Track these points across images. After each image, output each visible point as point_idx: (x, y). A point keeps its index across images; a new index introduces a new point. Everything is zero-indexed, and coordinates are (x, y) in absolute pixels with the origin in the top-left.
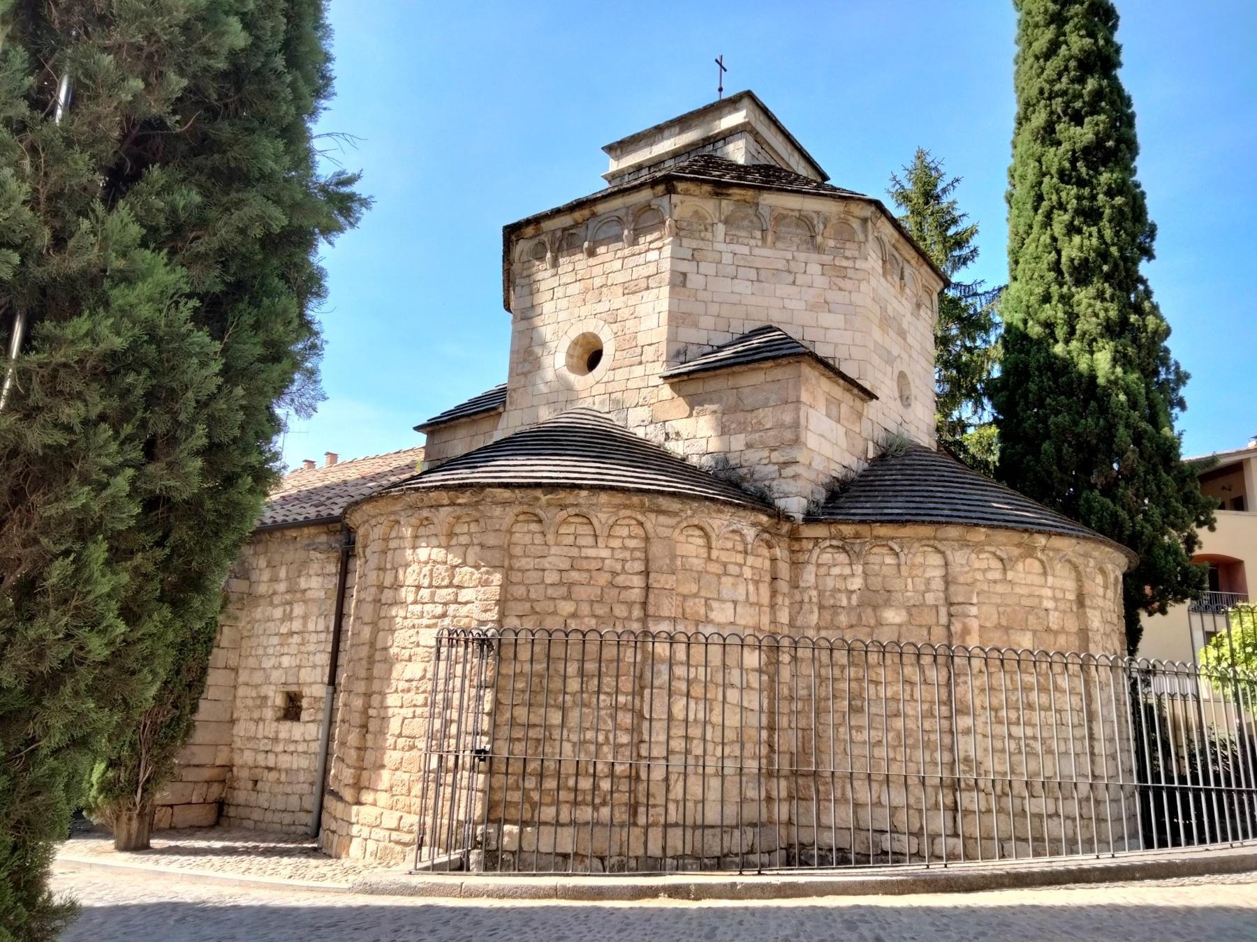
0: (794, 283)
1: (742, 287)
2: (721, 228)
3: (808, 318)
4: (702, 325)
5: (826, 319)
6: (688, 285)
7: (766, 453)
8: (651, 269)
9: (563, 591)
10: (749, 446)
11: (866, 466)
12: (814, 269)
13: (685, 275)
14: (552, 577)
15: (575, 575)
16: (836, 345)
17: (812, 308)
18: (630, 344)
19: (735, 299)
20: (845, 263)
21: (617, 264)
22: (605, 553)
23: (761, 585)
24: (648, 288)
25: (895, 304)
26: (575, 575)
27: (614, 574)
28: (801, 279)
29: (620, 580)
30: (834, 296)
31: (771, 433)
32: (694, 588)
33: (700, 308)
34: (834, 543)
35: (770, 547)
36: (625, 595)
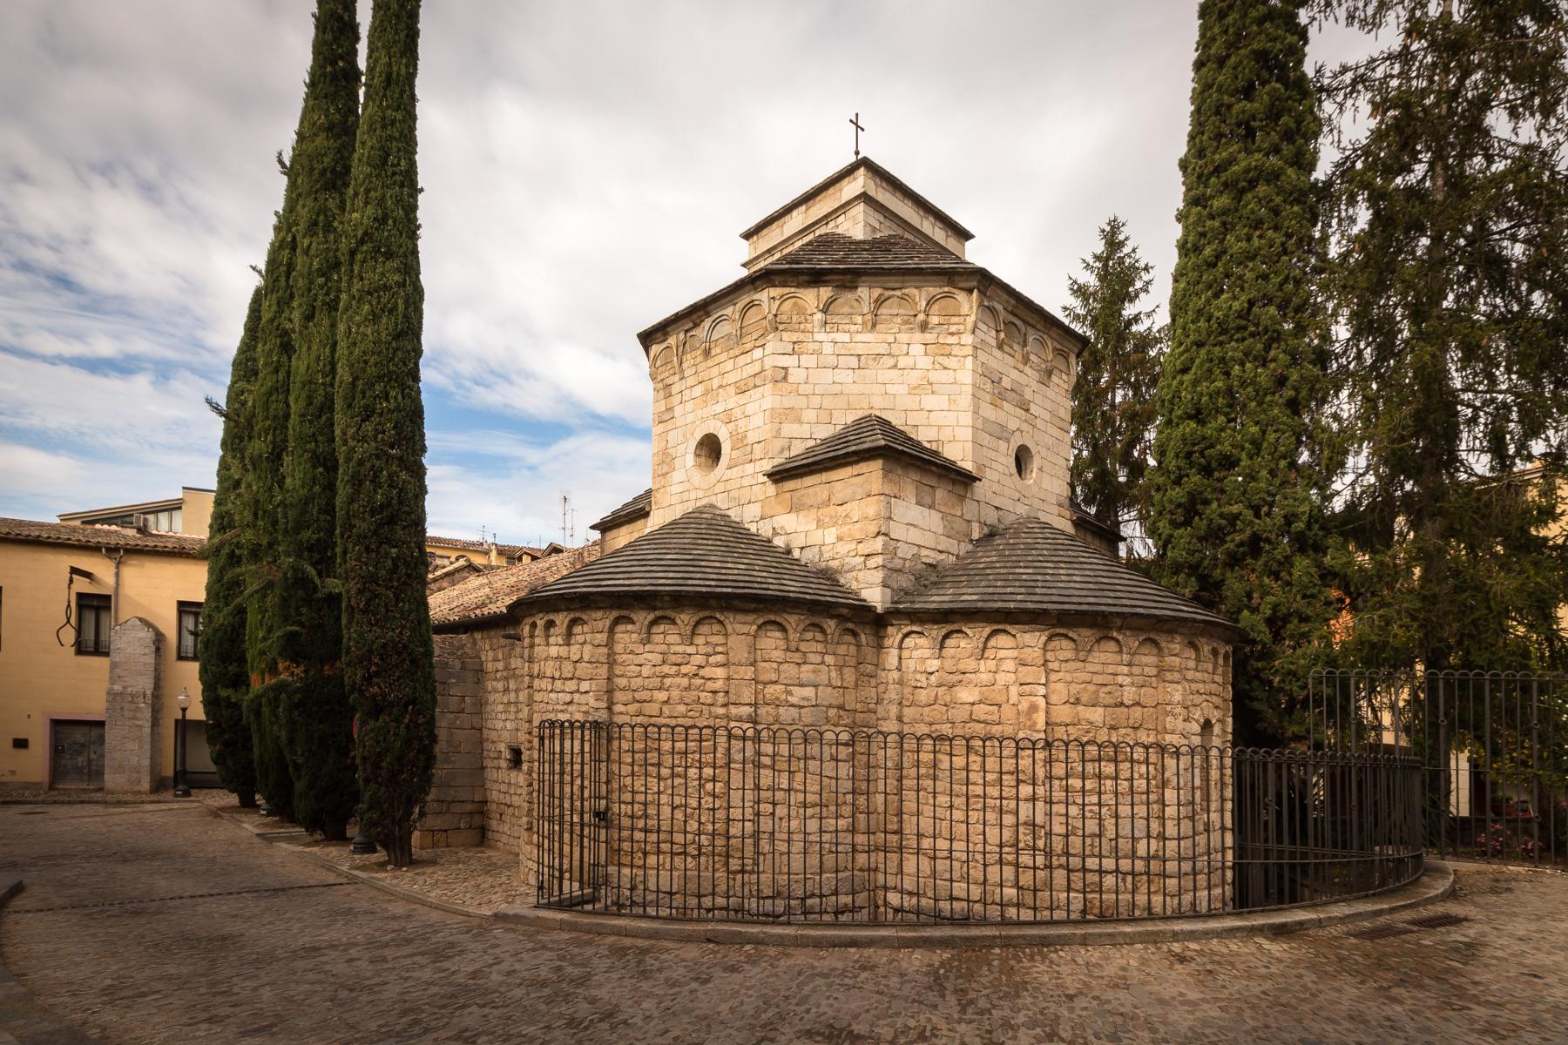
1: (845, 376)
3: (910, 402)
4: (805, 419)
5: (929, 401)
6: (791, 379)
7: (853, 546)
8: (756, 368)
9: (656, 682)
10: (840, 539)
13: (786, 369)
14: (646, 671)
15: (666, 669)
16: (939, 427)
18: (740, 440)
19: (837, 388)
21: (729, 365)
24: (756, 386)
25: (1015, 374)
26: (666, 669)
27: (700, 667)
28: (902, 362)
29: (705, 672)
31: (857, 526)
32: (774, 677)
33: (802, 402)
34: (915, 628)
35: (855, 634)
36: (710, 685)
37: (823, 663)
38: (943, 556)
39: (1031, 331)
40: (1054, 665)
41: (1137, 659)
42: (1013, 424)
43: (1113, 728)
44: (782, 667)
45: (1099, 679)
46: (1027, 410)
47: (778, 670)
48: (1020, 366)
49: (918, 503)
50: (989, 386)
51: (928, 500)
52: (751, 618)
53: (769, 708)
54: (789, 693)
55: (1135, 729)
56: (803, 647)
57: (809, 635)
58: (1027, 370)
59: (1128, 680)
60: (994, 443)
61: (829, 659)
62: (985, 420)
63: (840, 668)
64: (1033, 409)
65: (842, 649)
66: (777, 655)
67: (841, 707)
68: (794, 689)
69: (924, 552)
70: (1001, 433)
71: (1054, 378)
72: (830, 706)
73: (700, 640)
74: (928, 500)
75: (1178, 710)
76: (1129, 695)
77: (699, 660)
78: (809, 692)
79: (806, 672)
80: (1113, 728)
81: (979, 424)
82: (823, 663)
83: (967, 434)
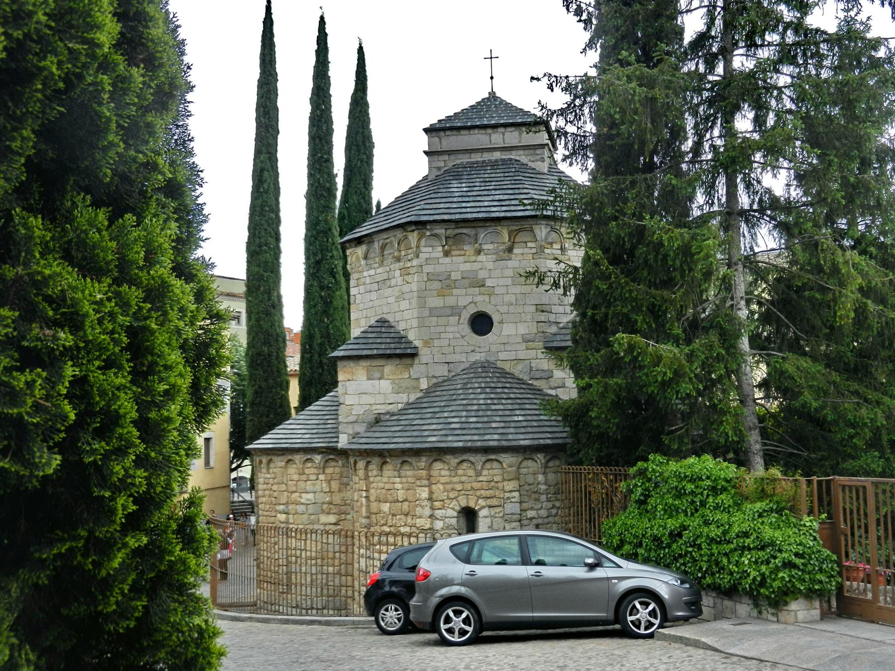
0: (390, 287)
1: (374, 296)
2: (363, 262)
3: (395, 308)
5: (404, 305)
11: (420, 395)
12: (398, 273)
17: (399, 299)
20: (409, 264)
22: (269, 476)
23: (333, 483)
30: (406, 288)
32: (294, 489)
37: (317, 479)
38: (391, 406)
39: (480, 230)
40: (371, 479)
41: (403, 473)
42: (462, 302)
43: (394, 515)
44: (299, 483)
45: (387, 486)
46: (483, 285)
47: (296, 485)
48: (473, 258)
49: (369, 379)
50: (436, 285)
51: (377, 375)
52: (282, 458)
53: (293, 506)
54: (301, 497)
55: (406, 515)
56: (307, 471)
57: (309, 465)
58: (482, 258)
59: (399, 486)
60: (443, 320)
61: (321, 477)
62: (431, 309)
63: (329, 482)
64: (489, 283)
65: (329, 470)
66: (296, 477)
67: (330, 503)
68: (303, 495)
69: (374, 407)
70: (455, 311)
71: (516, 251)
72: (323, 503)
73: (271, 471)
74: (377, 375)
75: (426, 503)
76: (401, 495)
77: (271, 481)
78: (310, 496)
79: (309, 486)
80: (394, 515)
81: (427, 313)
82: (317, 479)
83: (415, 323)
